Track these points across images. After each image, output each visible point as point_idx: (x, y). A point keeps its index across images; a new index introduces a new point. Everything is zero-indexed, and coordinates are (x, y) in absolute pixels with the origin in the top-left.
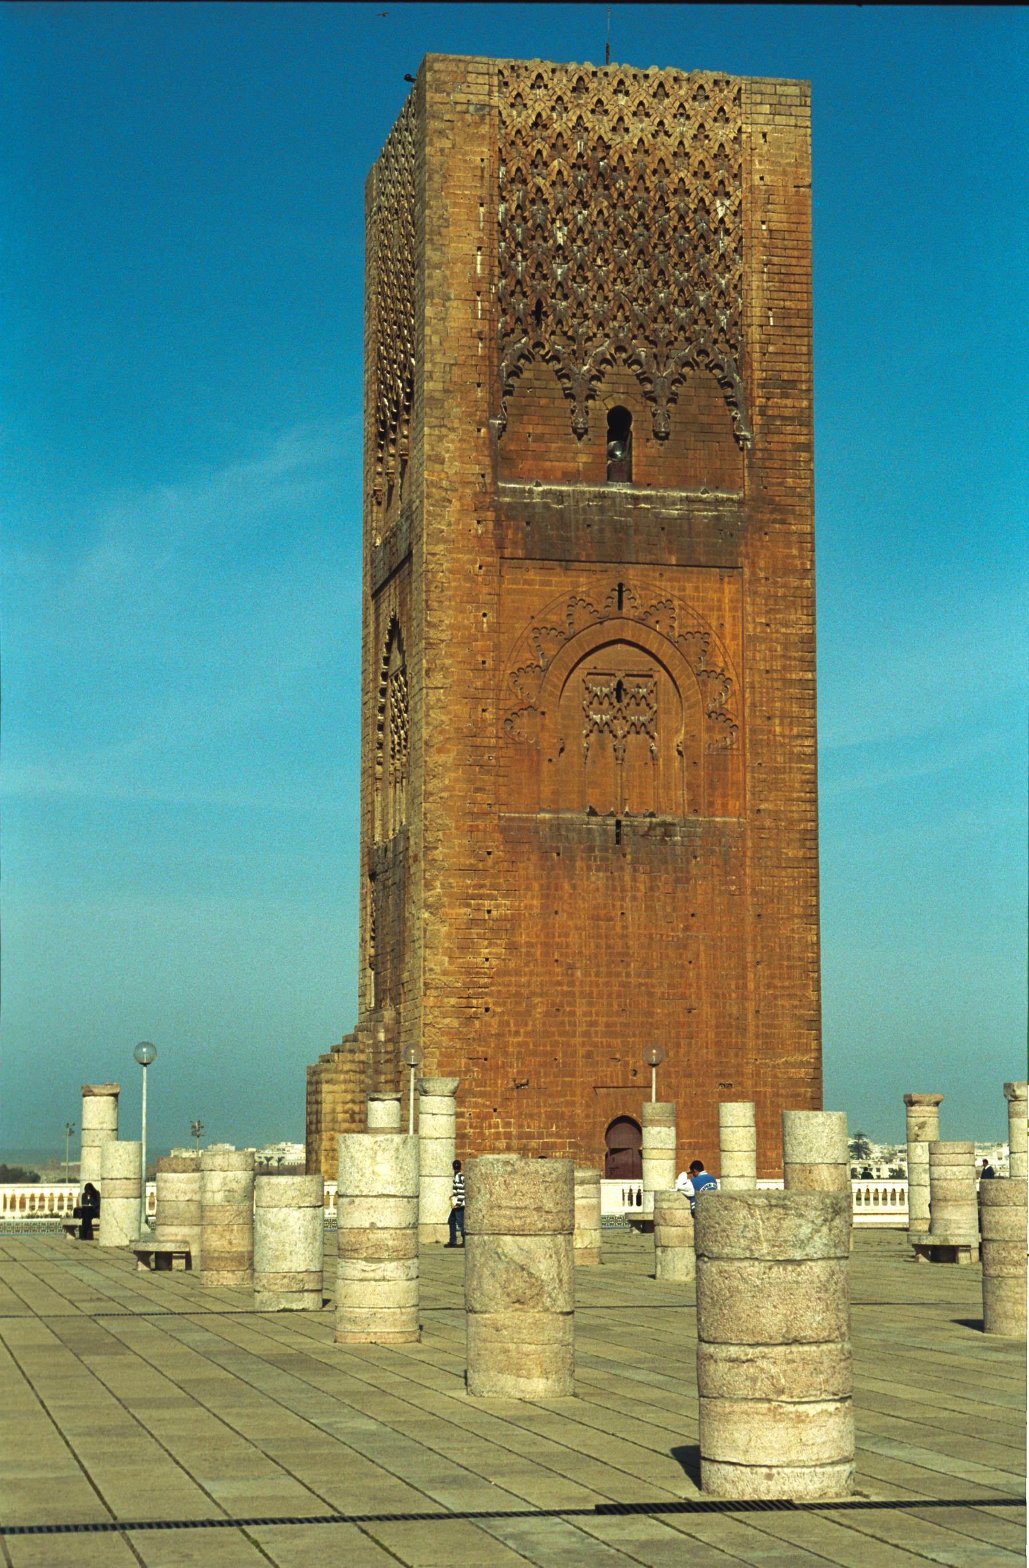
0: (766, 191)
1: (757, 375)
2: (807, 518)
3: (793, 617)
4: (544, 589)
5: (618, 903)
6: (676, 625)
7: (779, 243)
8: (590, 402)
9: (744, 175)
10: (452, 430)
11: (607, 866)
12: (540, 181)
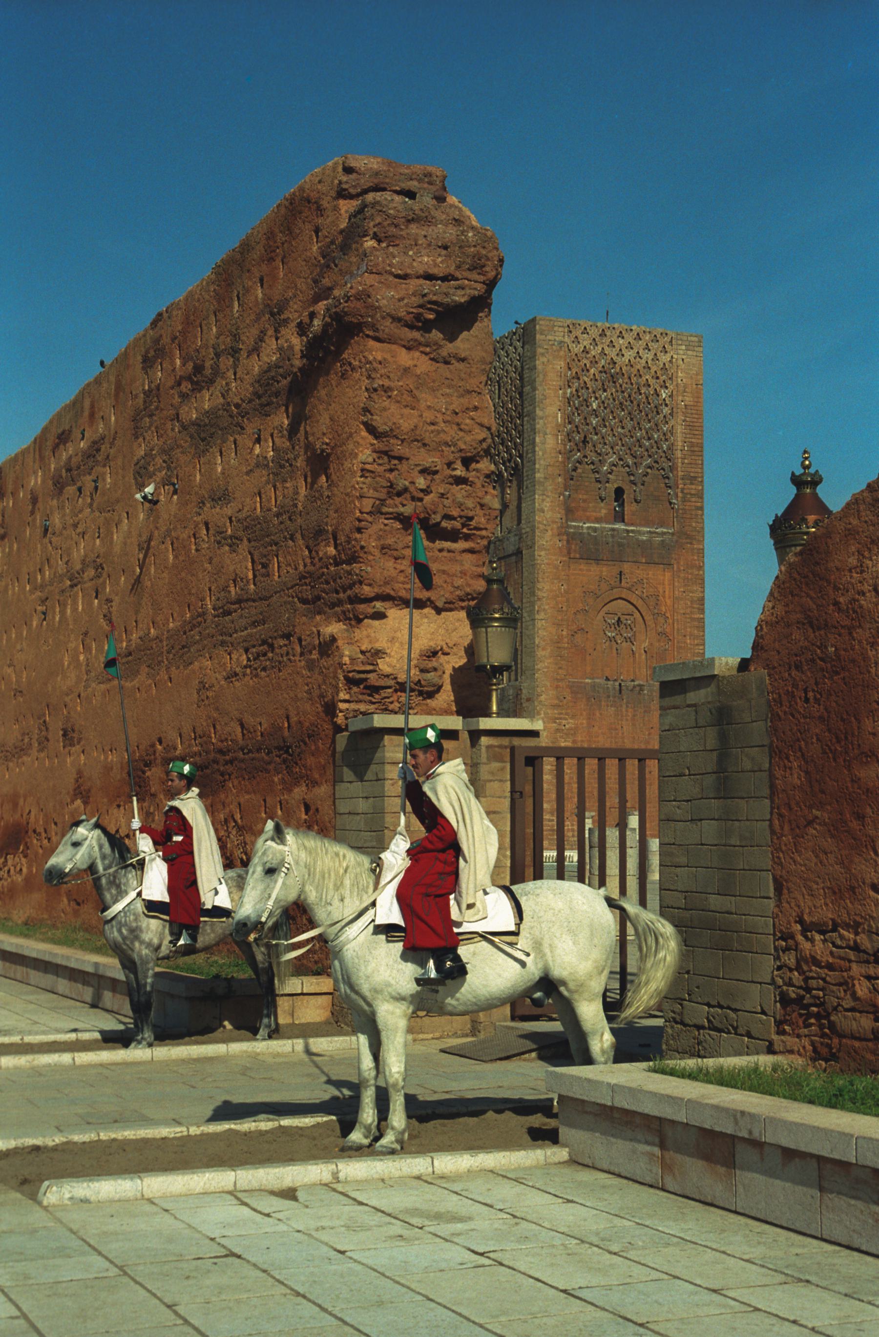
1: (680, 474)
2: (701, 542)
4: (590, 574)
7: (689, 411)
8: (607, 485)
10: (548, 496)
12: (586, 379)
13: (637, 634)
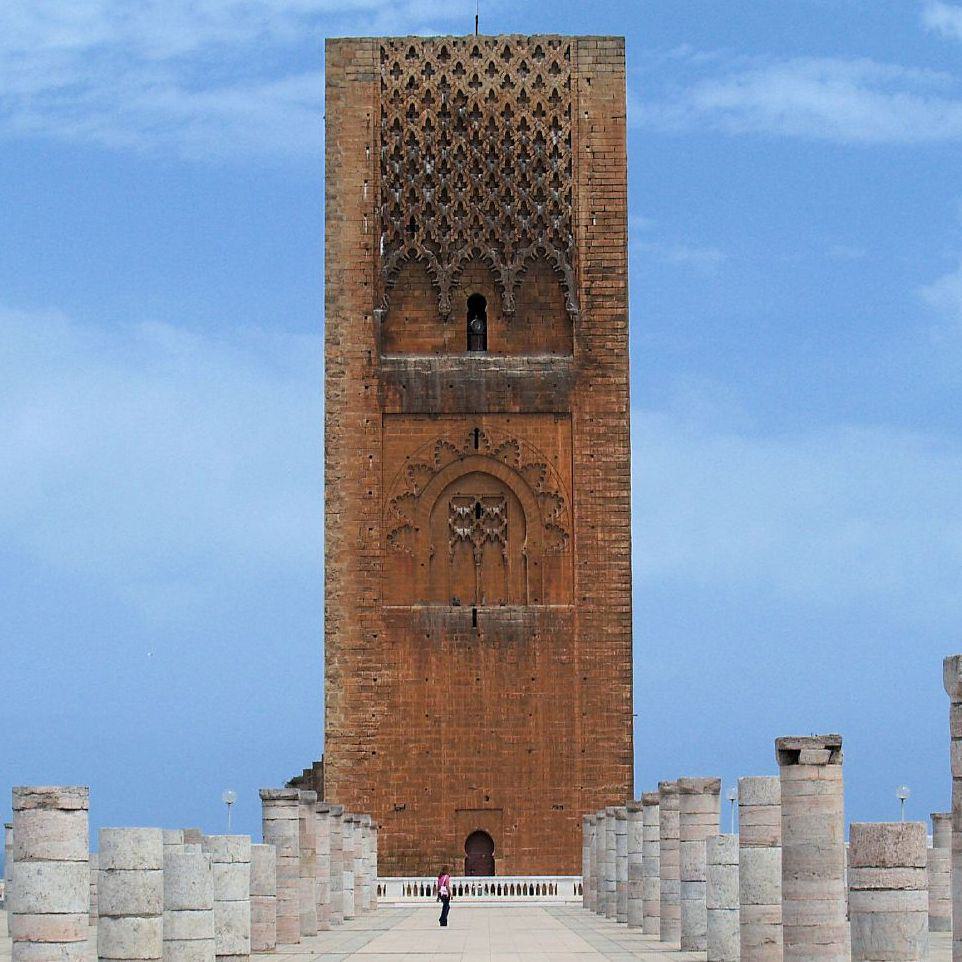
0: (589, 123)
6: (519, 459)
7: (600, 162)
9: (573, 110)
11: (466, 645)
13: (510, 528)
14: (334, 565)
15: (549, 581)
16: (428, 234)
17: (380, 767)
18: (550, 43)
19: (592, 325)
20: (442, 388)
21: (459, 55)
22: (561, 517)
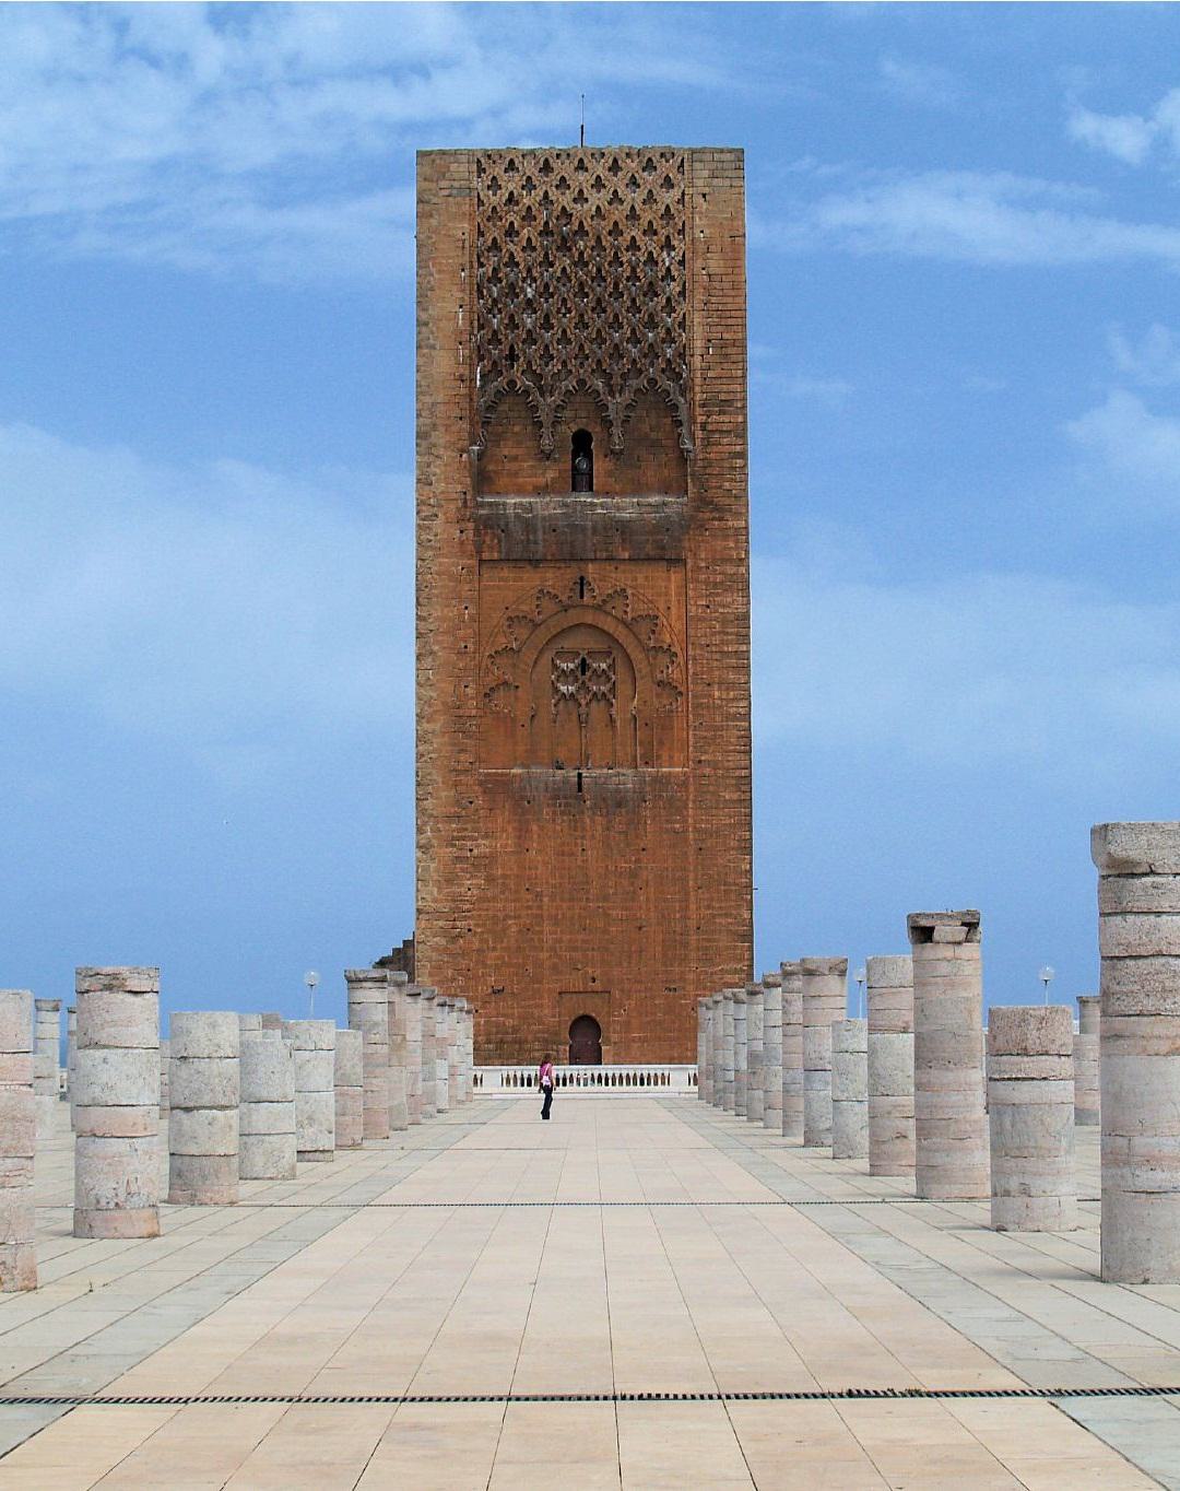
1: (698, 397)
2: (743, 514)
3: (729, 600)
5: (579, 841)
6: (628, 610)
12: (511, 247)
14: (426, 726)
15: (661, 743)
16: (529, 364)
17: (476, 945)
18: (662, 155)
19: (708, 463)
20: (544, 533)
21: (563, 168)
22: (675, 674)
